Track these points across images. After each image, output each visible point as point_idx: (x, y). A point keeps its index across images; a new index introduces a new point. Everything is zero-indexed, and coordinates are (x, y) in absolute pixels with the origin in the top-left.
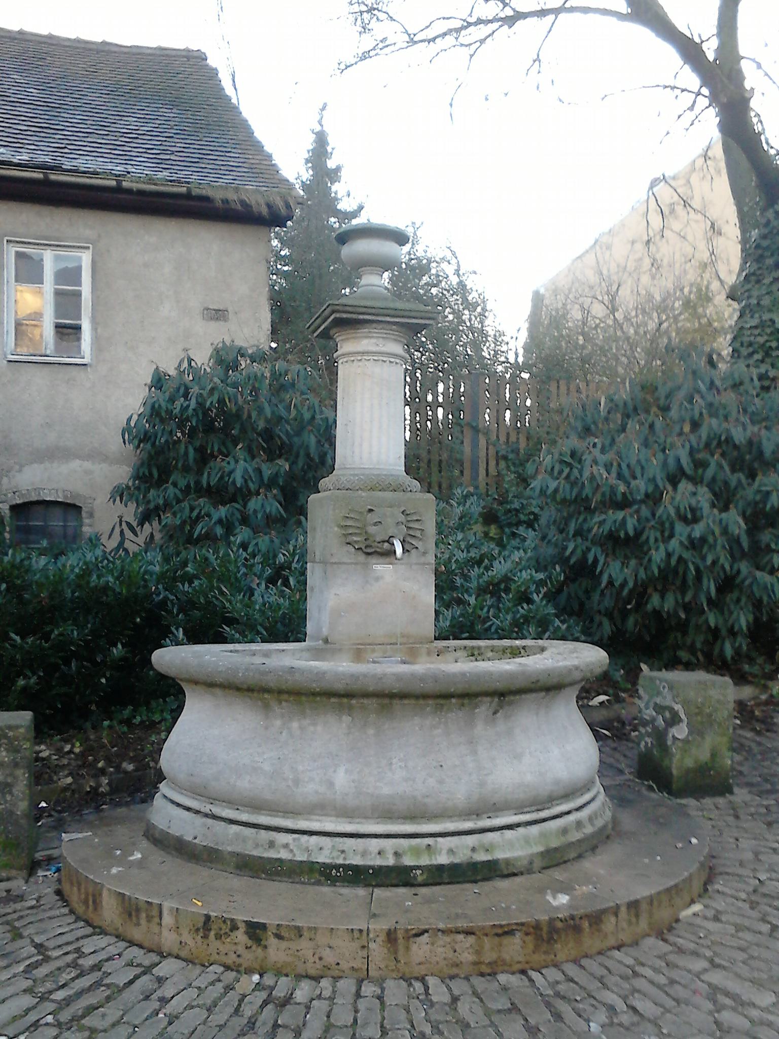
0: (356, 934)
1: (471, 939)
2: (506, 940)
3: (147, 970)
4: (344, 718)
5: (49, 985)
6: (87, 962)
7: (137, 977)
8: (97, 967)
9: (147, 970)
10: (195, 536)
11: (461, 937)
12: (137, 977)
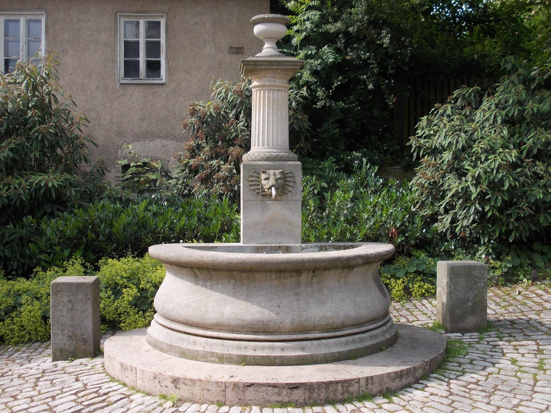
0: (220, 384)
1: (276, 390)
2: (295, 391)
3: (128, 396)
4: (231, 281)
5: (83, 399)
6: (102, 392)
7: (121, 399)
8: (105, 394)
9: (128, 396)
10: (54, 198)
11: (270, 389)
12: (121, 399)
